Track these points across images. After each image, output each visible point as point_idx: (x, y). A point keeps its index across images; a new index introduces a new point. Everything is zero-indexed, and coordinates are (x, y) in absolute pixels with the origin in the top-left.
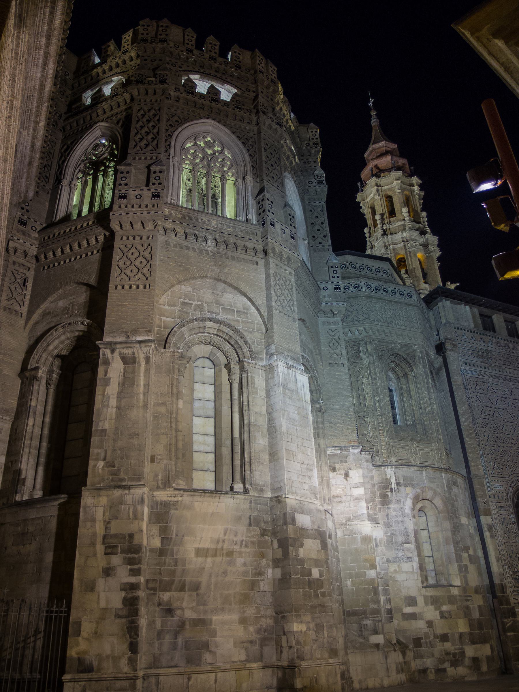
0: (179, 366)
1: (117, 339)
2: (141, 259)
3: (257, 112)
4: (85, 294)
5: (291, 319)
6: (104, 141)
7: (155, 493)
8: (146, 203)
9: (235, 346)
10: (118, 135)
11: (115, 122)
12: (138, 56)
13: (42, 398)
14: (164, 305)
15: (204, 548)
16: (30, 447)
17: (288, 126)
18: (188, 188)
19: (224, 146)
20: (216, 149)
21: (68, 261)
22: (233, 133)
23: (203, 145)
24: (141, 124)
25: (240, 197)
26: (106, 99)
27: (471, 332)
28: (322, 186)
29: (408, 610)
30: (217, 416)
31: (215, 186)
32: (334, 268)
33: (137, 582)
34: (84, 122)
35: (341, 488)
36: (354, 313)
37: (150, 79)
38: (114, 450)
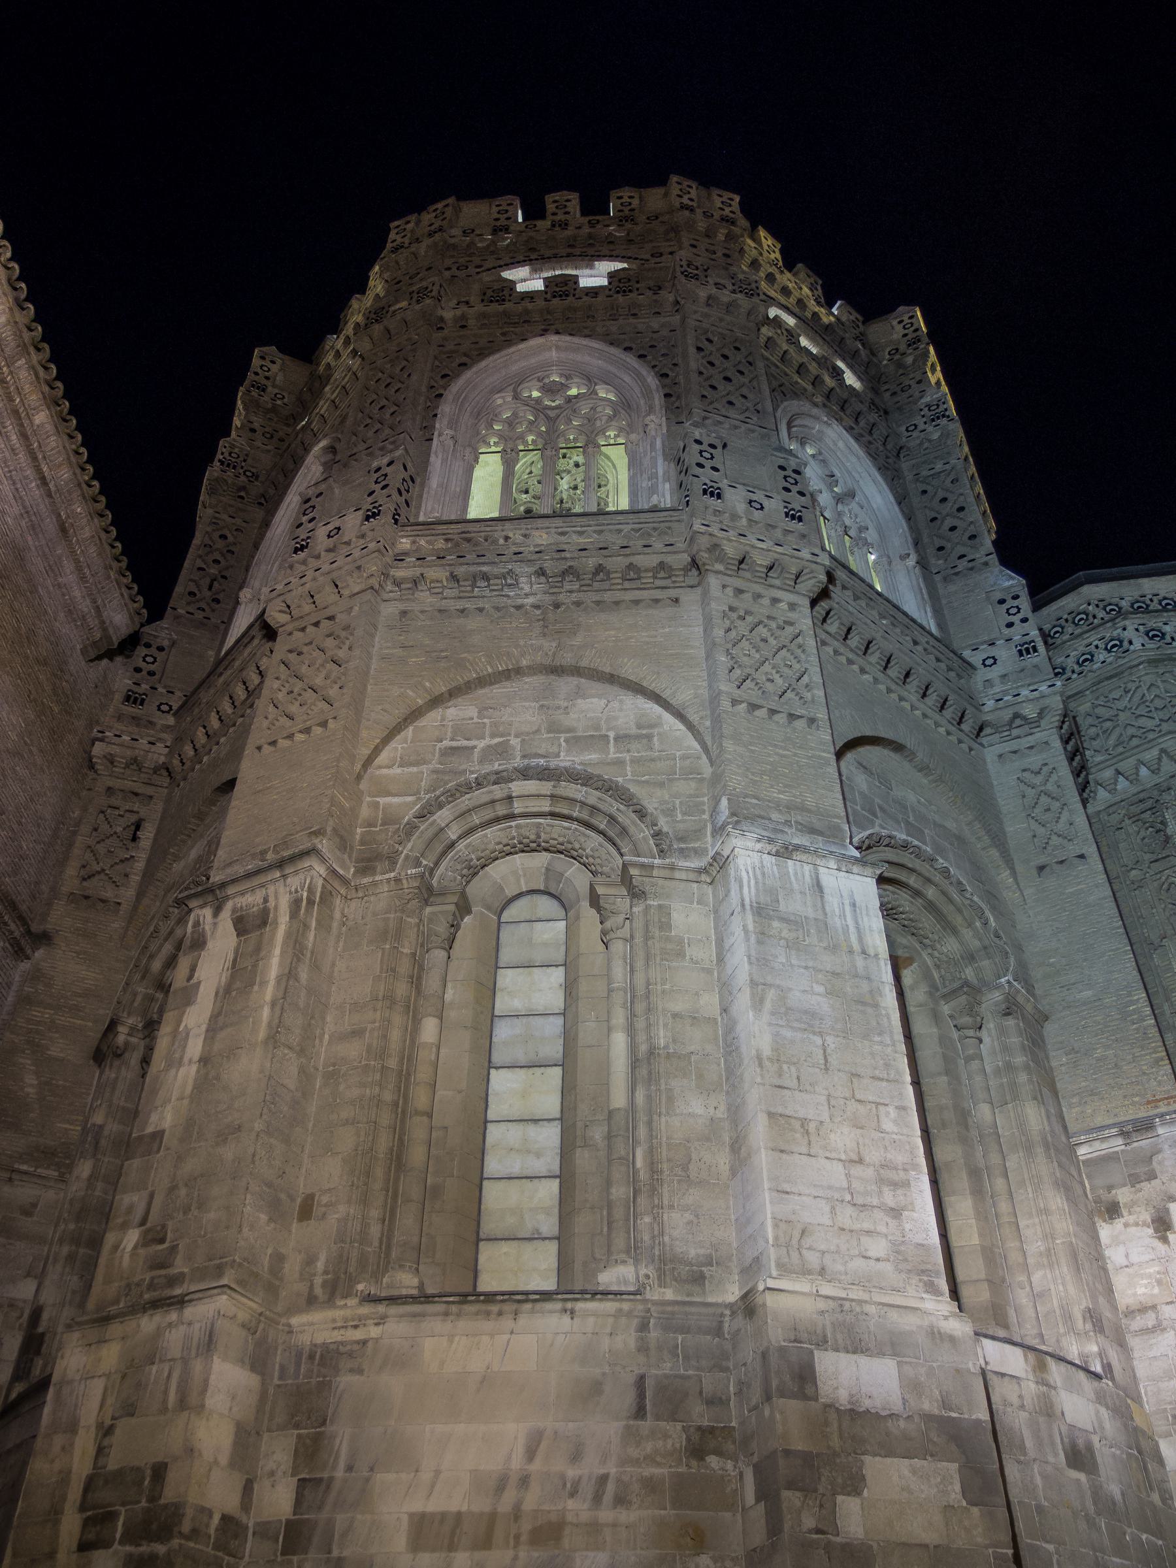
7: (295, 1321)
9: (611, 833)
15: (443, 1516)
17: (808, 315)
20: (574, 392)
23: (536, 394)
35: (1150, 1276)
38: (173, 1188)
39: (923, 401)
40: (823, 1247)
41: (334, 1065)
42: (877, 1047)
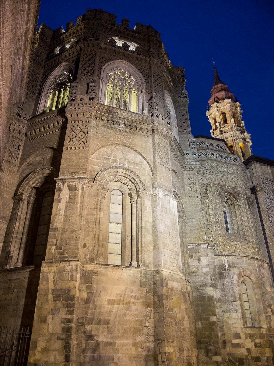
0: (102, 193)
1: (66, 177)
2: (82, 133)
3: (150, 56)
4: (50, 153)
5: (167, 169)
6: (65, 73)
7: (85, 266)
8: (85, 103)
9: (134, 183)
10: (73, 68)
11: (72, 62)
12: (85, 28)
13: (24, 211)
14: (94, 159)
15: (113, 300)
16: (16, 239)
17: (167, 66)
18: (111, 97)
19: (131, 74)
20: (126, 76)
21: (42, 135)
22: (136, 67)
23: (119, 74)
24: (85, 62)
25: (139, 102)
26: (67, 50)
27: (271, 181)
28: (186, 99)
29: (236, 341)
30: (123, 223)
31: (126, 97)
32: (193, 143)
33: (71, 318)
34: (55, 63)
36: (204, 169)
37: (91, 38)
38: (62, 240)
42: (176, 232)
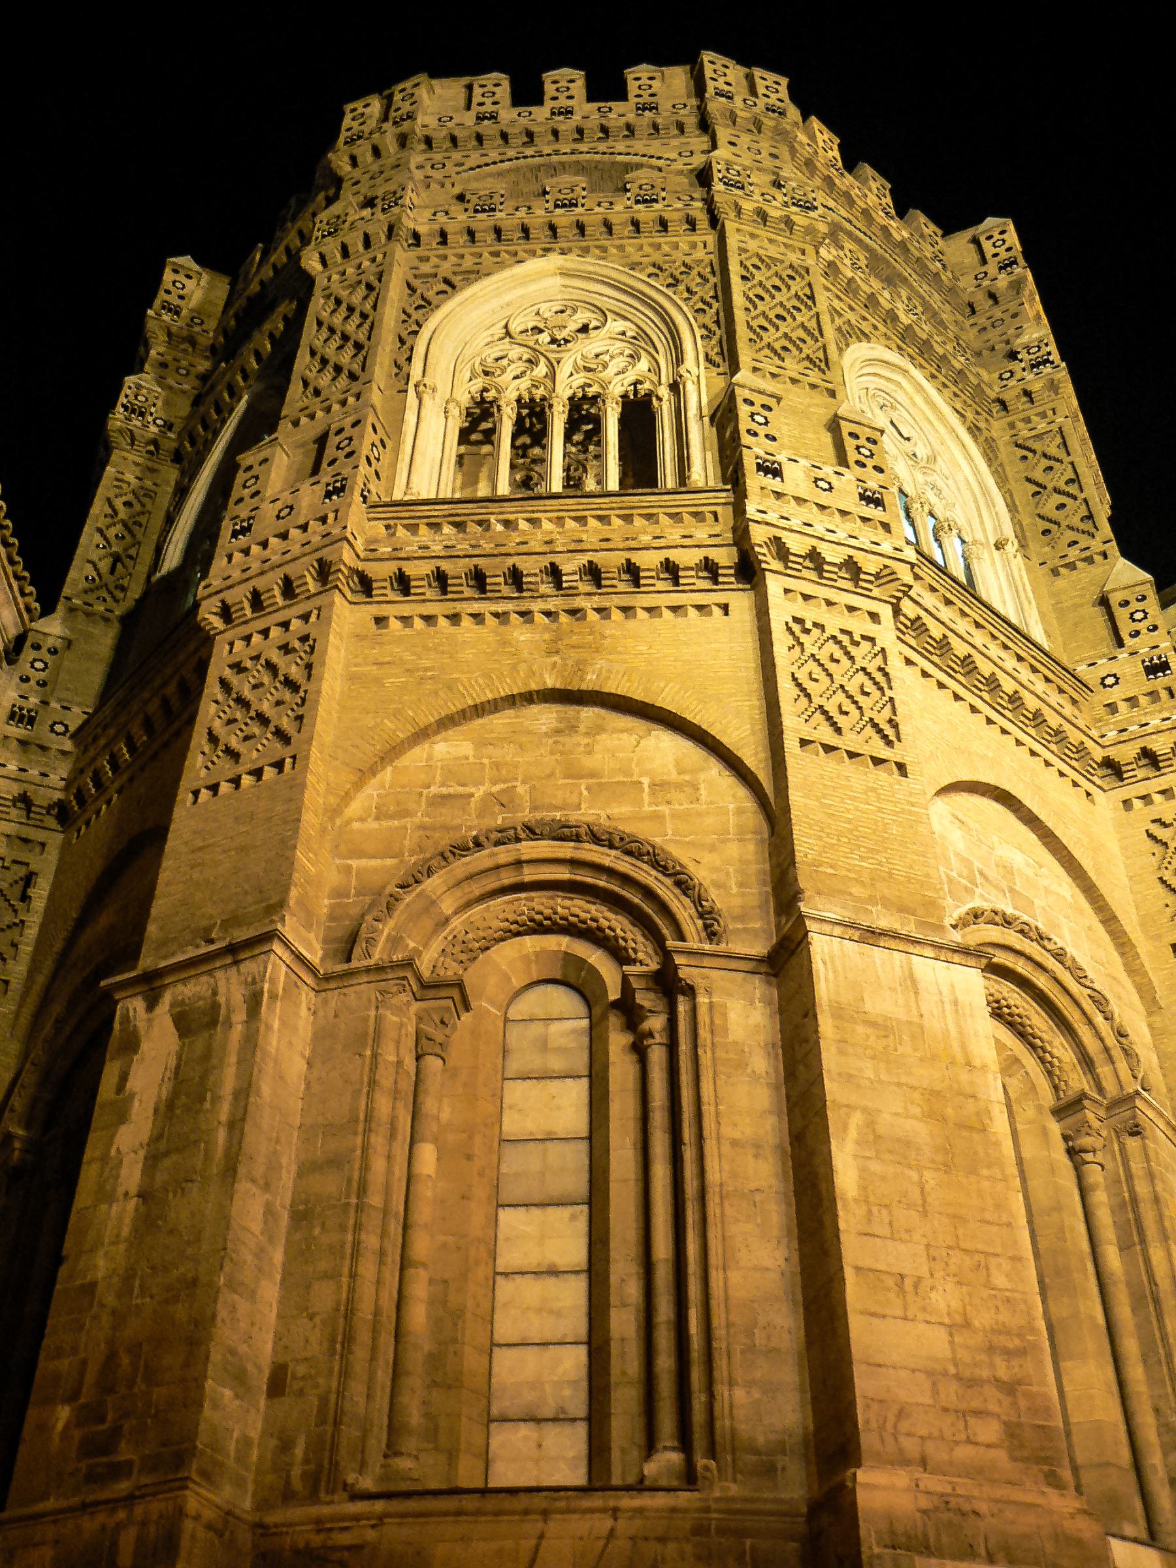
38: (111, 1358)
39: (1019, 341)
40: (923, 1432)
41: (306, 1202)
42: (986, 1184)
